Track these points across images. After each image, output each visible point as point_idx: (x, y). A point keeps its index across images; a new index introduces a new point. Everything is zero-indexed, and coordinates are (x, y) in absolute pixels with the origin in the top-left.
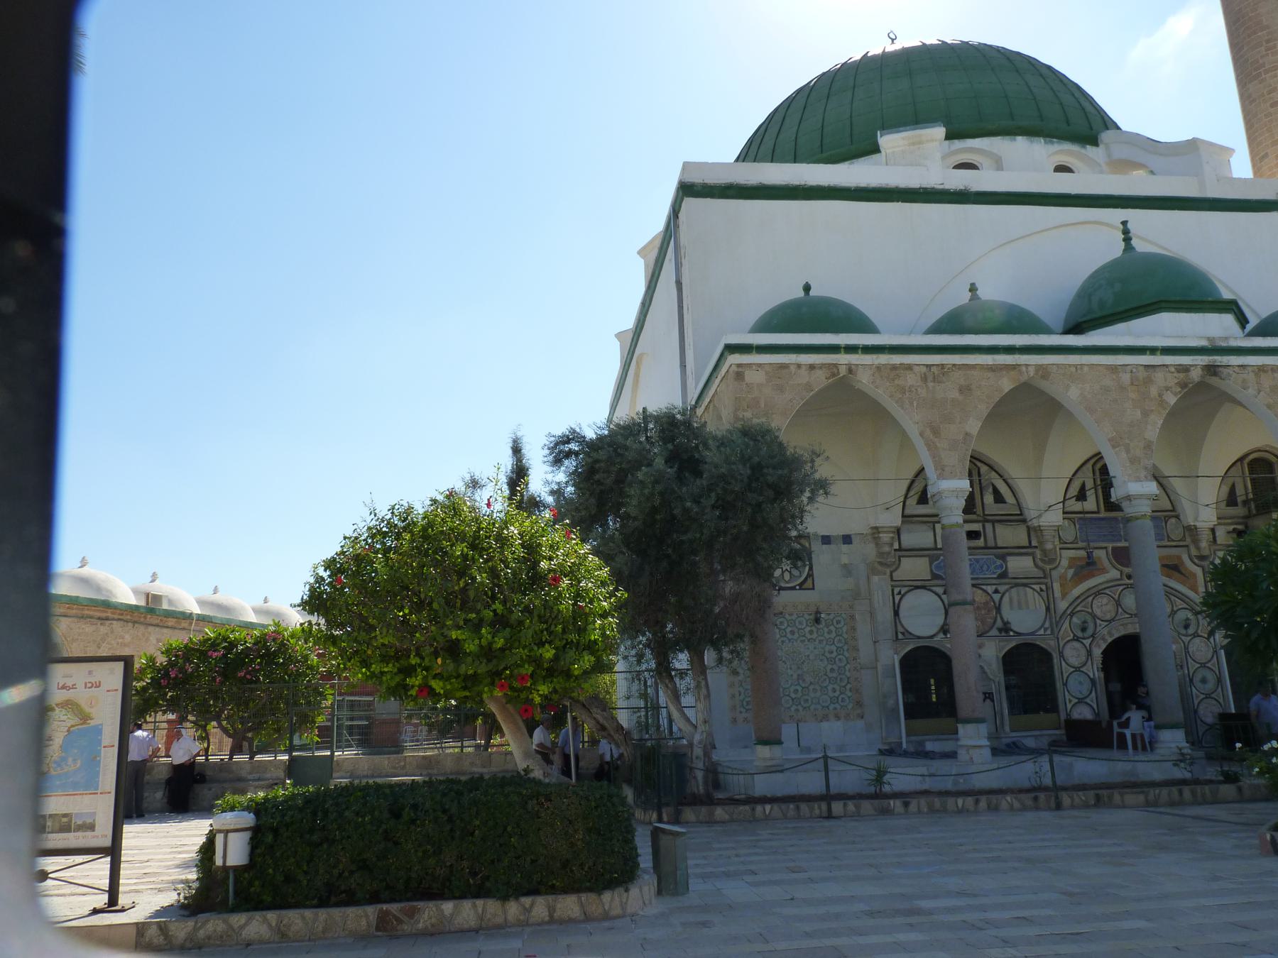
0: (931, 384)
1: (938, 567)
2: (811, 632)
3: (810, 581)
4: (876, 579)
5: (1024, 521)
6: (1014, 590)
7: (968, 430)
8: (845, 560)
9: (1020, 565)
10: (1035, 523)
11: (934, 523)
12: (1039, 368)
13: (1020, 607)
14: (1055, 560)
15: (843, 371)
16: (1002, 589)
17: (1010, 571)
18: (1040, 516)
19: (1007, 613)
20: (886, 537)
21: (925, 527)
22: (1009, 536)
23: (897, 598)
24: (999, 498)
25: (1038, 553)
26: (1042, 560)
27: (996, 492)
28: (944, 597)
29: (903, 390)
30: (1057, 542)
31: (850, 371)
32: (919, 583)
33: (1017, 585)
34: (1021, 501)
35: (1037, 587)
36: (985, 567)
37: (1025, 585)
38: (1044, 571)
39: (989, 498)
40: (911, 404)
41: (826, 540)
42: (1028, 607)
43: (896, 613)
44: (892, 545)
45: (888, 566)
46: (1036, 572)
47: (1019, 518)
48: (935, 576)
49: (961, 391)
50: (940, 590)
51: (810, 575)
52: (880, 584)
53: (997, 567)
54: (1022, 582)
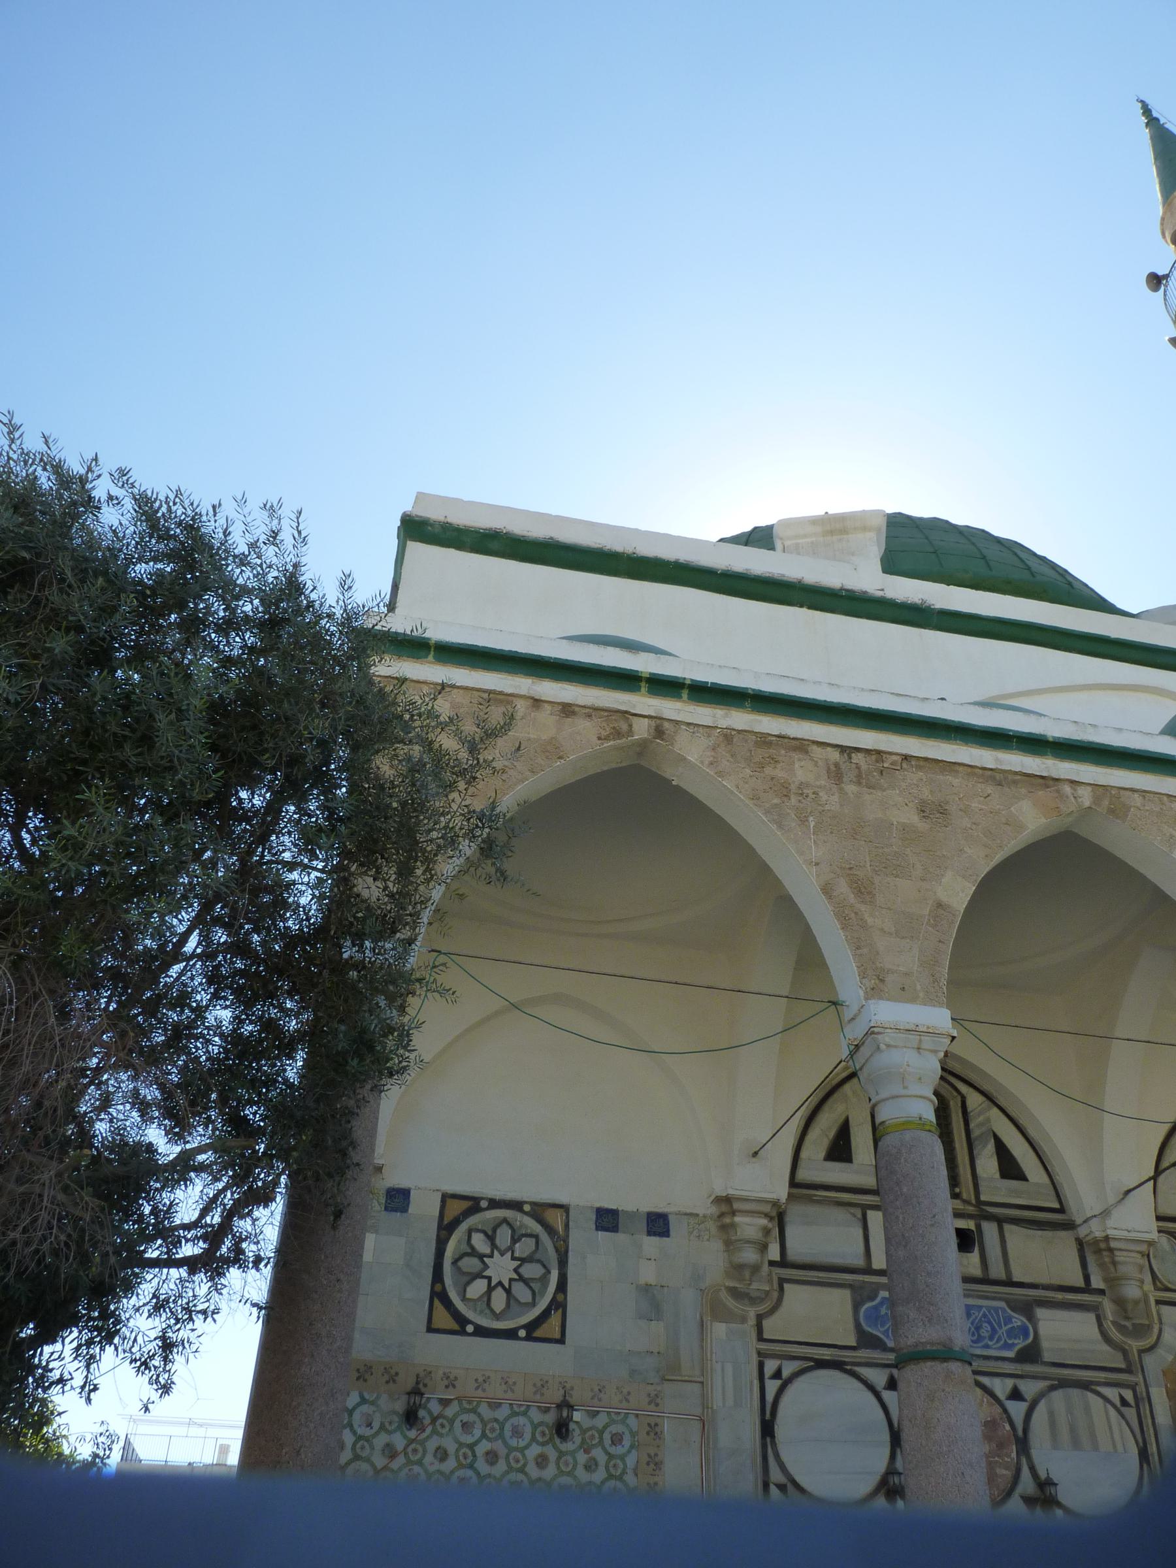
0: (851, 789)
1: (875, 1317)
2: (542, 1461)
3: (555, 1319)
4: (720, 1330)
5: (1070, 1226)
6: (1057, 1395)
7: (942, 895)
8: (648, 1274)
9: (1066, 1332)
10: (1095, 1230)
11: (864, 1208)
12: (1100, 790)
13: (1076, 1444)
14: (1149, 1327)
15: (642, 729)
16: (1029, 1388)
17: (1045, 1344)
18: (1105, 1213)
19: (1050, 1459)
20: (749, 1226)
21: (840, 1214)
22: (1039, 1258)
23: (772, 1387)
24: (1010, 1168)
25: (1108, 1307)
26: (1114, 1323)
27: (1002, 1151)
28: (888, 1396)
29: (784, 790)
30: (1148, 1286)
31: (659, 732)
32: (826, 1354)
33: (1063, 1384)
34: (1060, 1178)
35: (1112, 1393)
36: (985, 1330)
37: (1086, 1386)
38: (1125, 1353)
39: (988, 1164)
40: (803, 821)
41: (608, 1220)
42: (1095, 1447)
43: (767, 1429)
44: (764, 1248)
45: (753, 1301)
46: (1105, 1355)
47: (1055, 1218)
48: (866, 1340)
49: (923, 810)
50: (878, 1377)
51: (558, 1304)
52: (730, 1349)
53: (1011, 1333)
54: (1072, 1378)
